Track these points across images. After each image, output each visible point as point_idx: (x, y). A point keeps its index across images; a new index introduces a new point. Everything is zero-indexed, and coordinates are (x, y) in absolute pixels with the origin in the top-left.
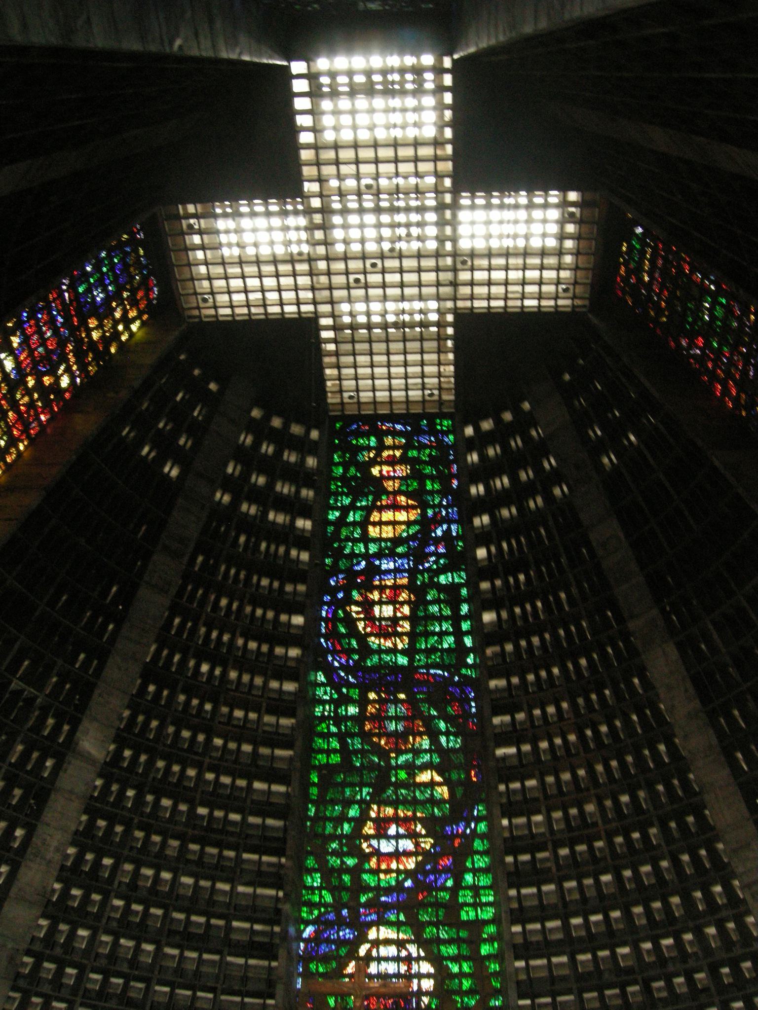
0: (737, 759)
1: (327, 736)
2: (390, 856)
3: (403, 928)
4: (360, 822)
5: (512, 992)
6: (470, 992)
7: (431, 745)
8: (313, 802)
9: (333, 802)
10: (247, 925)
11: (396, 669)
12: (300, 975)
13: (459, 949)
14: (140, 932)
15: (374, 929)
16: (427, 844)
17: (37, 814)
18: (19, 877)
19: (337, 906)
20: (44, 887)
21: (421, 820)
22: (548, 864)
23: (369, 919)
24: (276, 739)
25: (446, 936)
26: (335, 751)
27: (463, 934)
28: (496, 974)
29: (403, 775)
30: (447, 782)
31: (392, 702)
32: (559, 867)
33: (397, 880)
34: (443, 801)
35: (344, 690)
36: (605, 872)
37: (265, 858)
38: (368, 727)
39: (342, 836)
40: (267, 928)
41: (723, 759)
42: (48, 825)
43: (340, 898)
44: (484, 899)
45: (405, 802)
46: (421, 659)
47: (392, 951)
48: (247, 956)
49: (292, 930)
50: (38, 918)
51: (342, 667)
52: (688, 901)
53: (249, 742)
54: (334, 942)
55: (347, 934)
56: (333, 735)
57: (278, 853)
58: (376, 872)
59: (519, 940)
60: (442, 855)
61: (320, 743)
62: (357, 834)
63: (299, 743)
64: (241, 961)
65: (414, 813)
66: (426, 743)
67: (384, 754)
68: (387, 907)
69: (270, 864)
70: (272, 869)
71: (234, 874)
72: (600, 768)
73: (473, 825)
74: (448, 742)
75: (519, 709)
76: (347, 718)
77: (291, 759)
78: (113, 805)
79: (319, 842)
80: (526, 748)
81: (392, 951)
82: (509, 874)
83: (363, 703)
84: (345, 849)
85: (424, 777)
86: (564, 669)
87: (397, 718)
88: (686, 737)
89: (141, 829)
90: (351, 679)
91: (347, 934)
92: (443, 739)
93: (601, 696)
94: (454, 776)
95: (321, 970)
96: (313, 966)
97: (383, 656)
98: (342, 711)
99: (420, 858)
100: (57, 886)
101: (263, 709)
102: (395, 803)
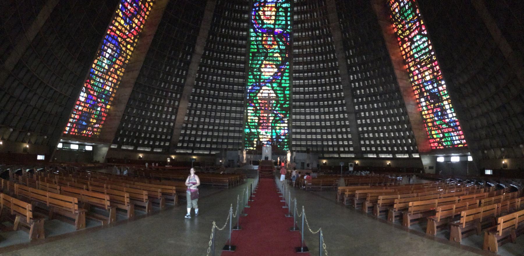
1: (253, 45)
2: (267, 72)
4: (261, 65)
6: (282, 100)
9: (255, 60)
10: (237, 87)
11: (271, 28)
16: (276, 70)
17: (188, 67)
19: (256, 82)
21: (275, 65)
24: (242, 46)
26: (256, 49)
27: (282, 89)
28: (288, 97)
29: (271, 54)
30: (281, 57)
31: (269, 37)
34: (280, 61)
37: (240, 73)
38: (263, 43)
39: (257, 68)
40: (241, 87)
45: (271, 60)
46: (277, 26)
47: (267, 91)
48: (237, 93)
49: (247, 87)
55: (258, 88)
56: (255, 45)
57: (243, 72)
59: (294, 91)
61: (252, 46)
62: (260, 67)
66: (276, 47)
67: (267, 49)
68: (267, 83)
71: (234, 77)
72: (317, 57)
76: (258, 41)
80: (301, 50)
81: (267, 91)
83: (262, 37)
87: (270, 41)
91: (258, 88)
92: (281, 47)
95: (253, 95)
98: (257, 39)
100: (195, 82)
102: (269, 61)
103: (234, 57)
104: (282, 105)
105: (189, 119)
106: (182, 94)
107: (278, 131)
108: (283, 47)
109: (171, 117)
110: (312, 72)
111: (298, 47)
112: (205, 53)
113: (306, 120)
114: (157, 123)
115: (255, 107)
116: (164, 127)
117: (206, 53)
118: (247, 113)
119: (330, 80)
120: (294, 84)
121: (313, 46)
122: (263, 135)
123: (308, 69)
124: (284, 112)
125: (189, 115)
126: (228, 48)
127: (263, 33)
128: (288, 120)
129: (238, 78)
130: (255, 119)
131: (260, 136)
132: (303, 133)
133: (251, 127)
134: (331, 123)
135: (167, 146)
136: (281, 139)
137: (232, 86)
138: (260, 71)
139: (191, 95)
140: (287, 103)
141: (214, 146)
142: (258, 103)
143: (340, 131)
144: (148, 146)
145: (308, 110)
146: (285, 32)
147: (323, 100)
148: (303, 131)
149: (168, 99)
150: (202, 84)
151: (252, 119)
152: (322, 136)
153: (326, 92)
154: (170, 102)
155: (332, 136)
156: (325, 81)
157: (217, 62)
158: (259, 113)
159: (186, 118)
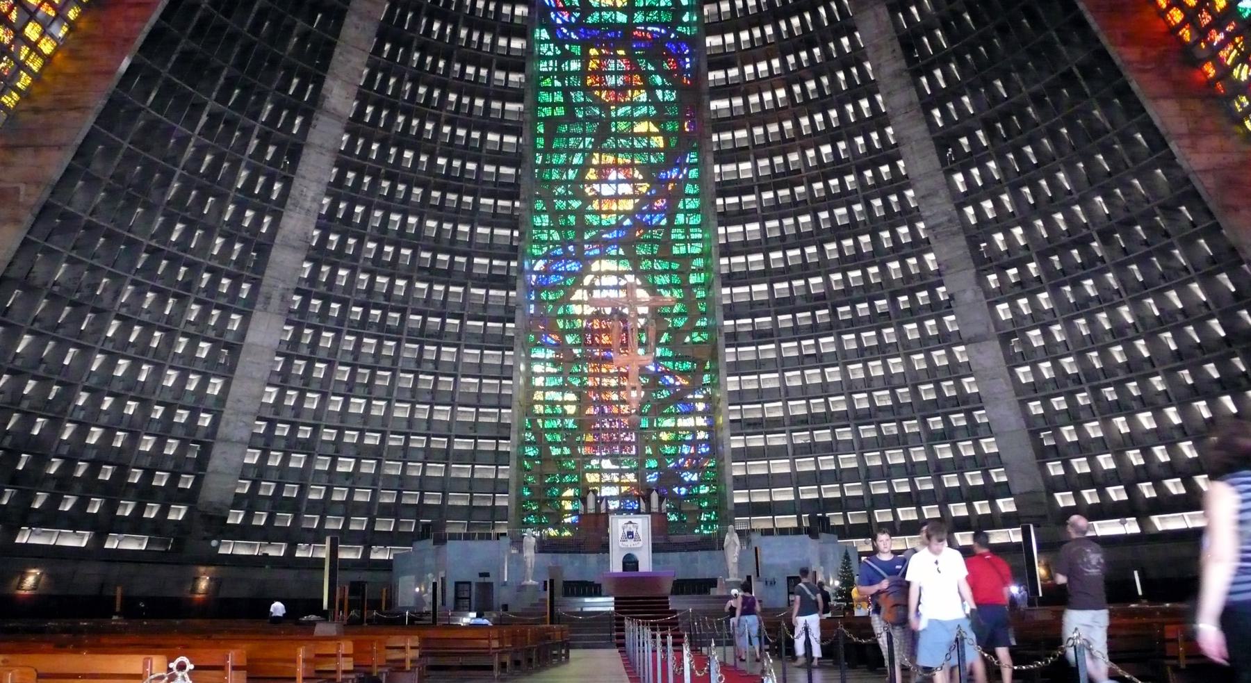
0: (932, 116)
2: (610, 198)
3: (622, 261)
4: (583, 168)
5: (719, 314)
6: (680, 314)
7: (648, 98)
8: (540, 151)
10: (486, 261)
11: (615, 26)
12: (532, 302)
13: (670, 278)
14: (393, 270)
15: (597, 262)
16: (644, 188)
18: (281, 225)
19: (564, 243)
20: (306, 233)
21: (639, 167)
22: (754, 206)
23: (592, 253)
24: (507, 94)
25: (660, 268)
27: (675, 266)
28: (702, 299)
29: (622, 126)
30: (663, 132)
32: (763, 209)
33: (617, 219)
34: (658, 150)
35: (567, 47)
36: (803, 213)
37: (500, 203)
38: (589, 82)
39: (567, 181)
40: (504, 263)
41: (922, 115)
42: (304, 177)
43: (567, 236)
44: (693, 236)
45: (623, 151)
46: (639, 18)
47: (612, 280)
48: (488, 288)
50: (303, 261)
51: (565, 24)
52: (876, 240)
53: (481, 97)
54: (561, 273)
55: (573, 266)
56: (557, 89)
57: (513, 197)
58: (598, 213)
60: (655, 198)
62: (580, 179)
63: (528, 98)
64: (482, 292)
65: (632, 160)
66: (643, 96)
67: (604, 107)
68: (608, 243)
69: (503, 207)
70: (505, 212)
71: (474, 217)
72: (805, 121)
73: (685, 171)
74: (664, 96)
75: (732, 65)
76: (570, 73)
77: (520, 113)
78: (359, 157)
79: (546, 187)
80: (738, 102)
81: (612, 280)
82: (720, 214)
83: (585, 58)
84: (570, 193)
85: (641, 127)
86: (777, 29)
87: (617, 73)
88: (889, 94)
89: (387, 179)
90: (574, 36)
91: (573, 266)
92: (659, 93)
93: (811, 55)
94: (669, 127)
95: (551, 298)
96: (543, 295)
97: (604, 13)
98: (565, 67)
99: (637, 201)
100: (316, 233)
101: (494, 66)
102: (615, 152)
103: (476, 135)
104: (675, 331)
105: (281, 397)
106: (261, 280)
107: (669, 450)
108: (671, 96)
109: (204, 384)
110: (791, 185)
111: (726, 90)
112: (360, 112)
113: (786, 394)
114: (131, 407)
115: (560, 346)
116: (164, 431)
117: (364, 114)
118: (530, 375)
119: (869, 207)
120: (723, 241)
121: (787, 79)
122: (600, 471)
123: (774, 175)
124: (687, 365)
125: (283, 381)
126: (453, 97)
127: (586, 46)
128: (708, 399)
129: (492, 225)
130: (563, 403)
131: (592, 478)
132: (778, 452)
133: (549, 437)
134: (894, 396)
135: (175, 522)
136: (681, 483)
137: (463, 260)
138: (579, 195)
139: (298, 291)
140: (701, 323)
141: (385, 525)
142: (571, 331)
143: (940, 426)
144: (75, 522)
145: (789, 348)
146: (673, 36)
147: (849, 295)
148: (777, 440)
149: (197, 302)
150: (342, 243)
151: (553, 404)
152: (861, 459)
153: (858, 260)
154: (204, 315)
155: (907, 455)
156: (851, 213)
157: (408, 154)
158: (581, 375)
159: (270, 398)
